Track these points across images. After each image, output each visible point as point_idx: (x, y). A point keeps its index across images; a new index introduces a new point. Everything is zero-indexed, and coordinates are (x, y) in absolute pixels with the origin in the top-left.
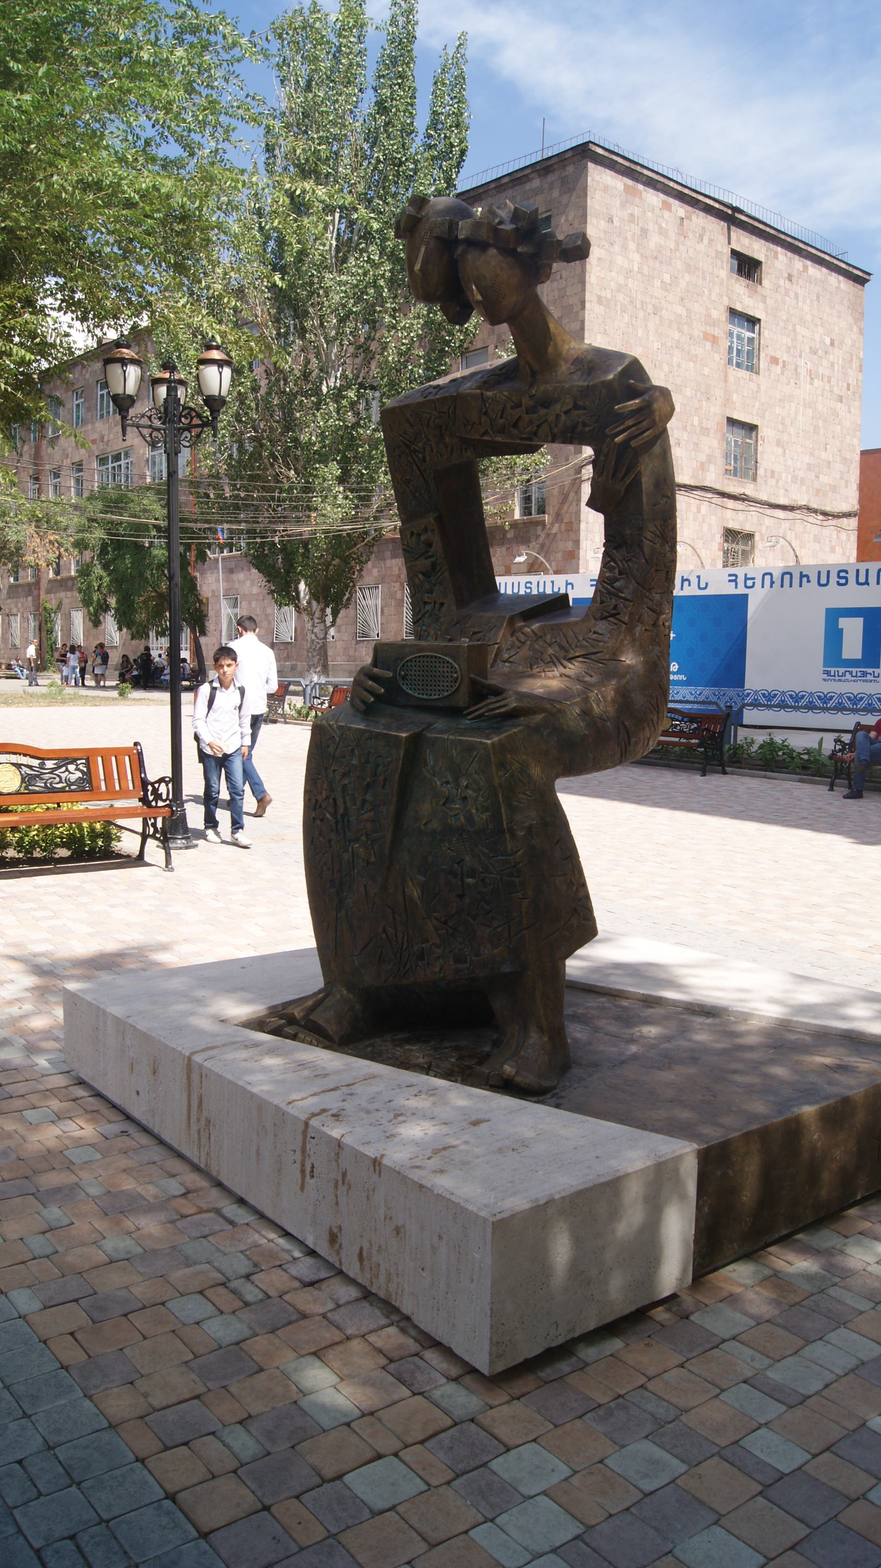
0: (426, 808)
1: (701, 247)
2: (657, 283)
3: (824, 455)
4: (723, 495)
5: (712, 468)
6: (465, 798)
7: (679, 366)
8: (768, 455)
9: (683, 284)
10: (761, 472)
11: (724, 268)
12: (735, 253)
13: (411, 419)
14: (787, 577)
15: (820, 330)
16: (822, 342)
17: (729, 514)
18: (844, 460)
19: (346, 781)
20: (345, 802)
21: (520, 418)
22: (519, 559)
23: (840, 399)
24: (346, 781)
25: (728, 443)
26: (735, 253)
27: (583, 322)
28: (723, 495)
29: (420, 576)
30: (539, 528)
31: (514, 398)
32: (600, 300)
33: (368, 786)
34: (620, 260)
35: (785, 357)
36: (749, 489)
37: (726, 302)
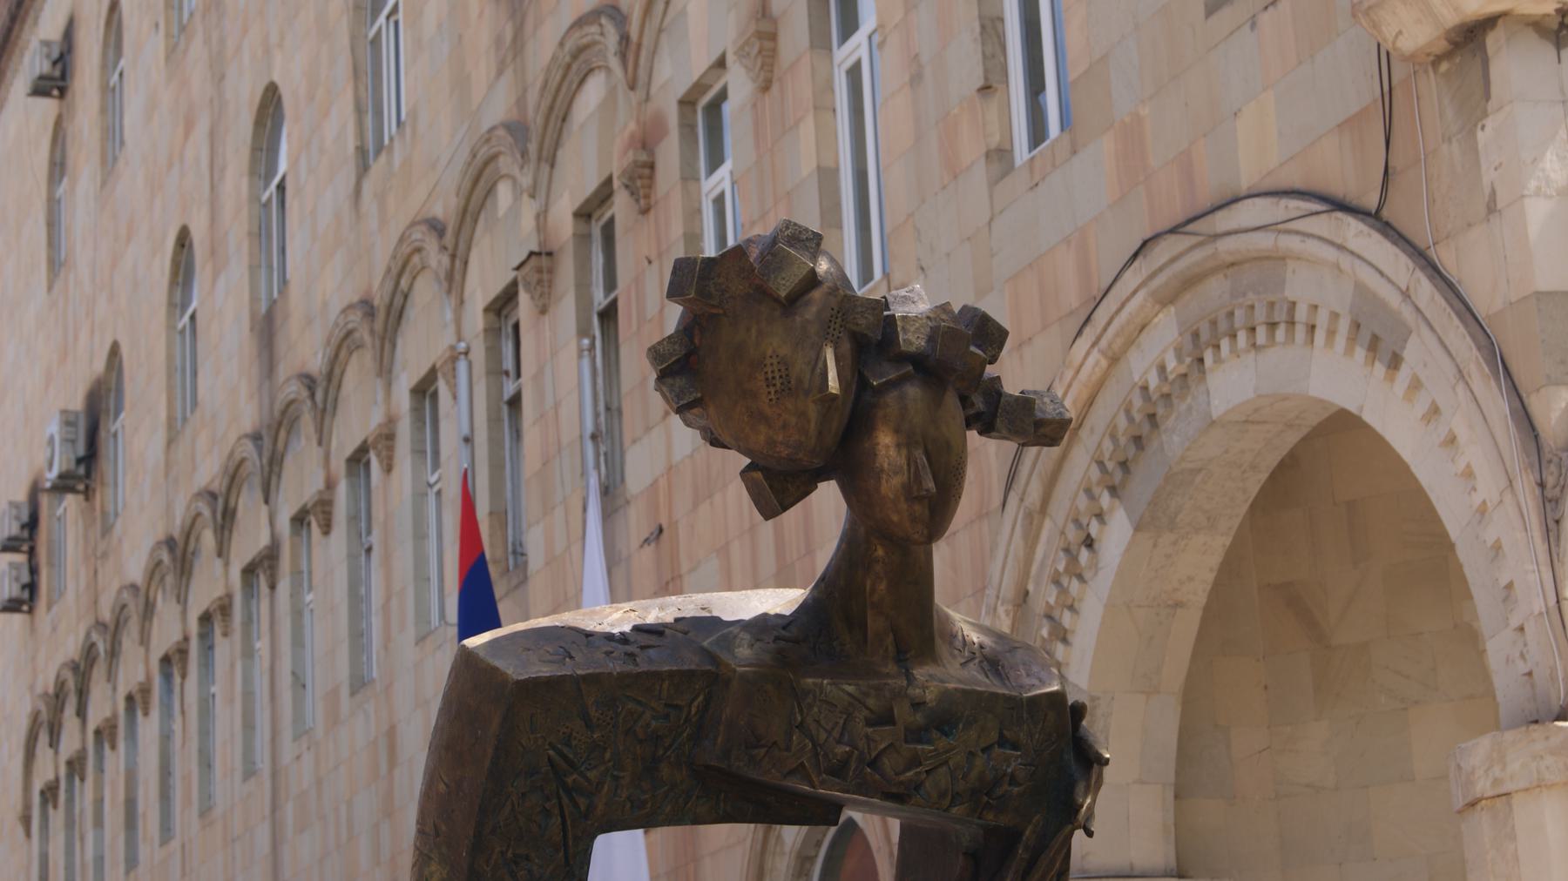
13: (593, 713)
21: (891, 745)
31: (871, 702)
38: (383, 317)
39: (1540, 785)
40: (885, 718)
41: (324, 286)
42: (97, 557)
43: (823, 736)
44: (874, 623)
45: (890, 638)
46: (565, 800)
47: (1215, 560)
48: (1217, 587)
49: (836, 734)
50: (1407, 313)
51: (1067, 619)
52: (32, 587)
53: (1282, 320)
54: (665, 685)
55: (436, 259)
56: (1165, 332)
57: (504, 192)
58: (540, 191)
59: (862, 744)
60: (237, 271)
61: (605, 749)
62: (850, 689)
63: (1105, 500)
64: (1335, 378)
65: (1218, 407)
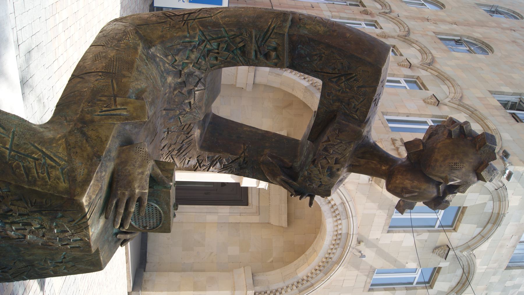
13: (363, 89)
21: (329, 162)
29: (241, 45)
31: (342, 159)
40: (337, 162)
43: (336, 147)
45: (357, 164)
46: (336, 75)
49: (336, 150)
54: (364, 110)
59: (332, 156)
61: (350, 90)
62: (347, 155)
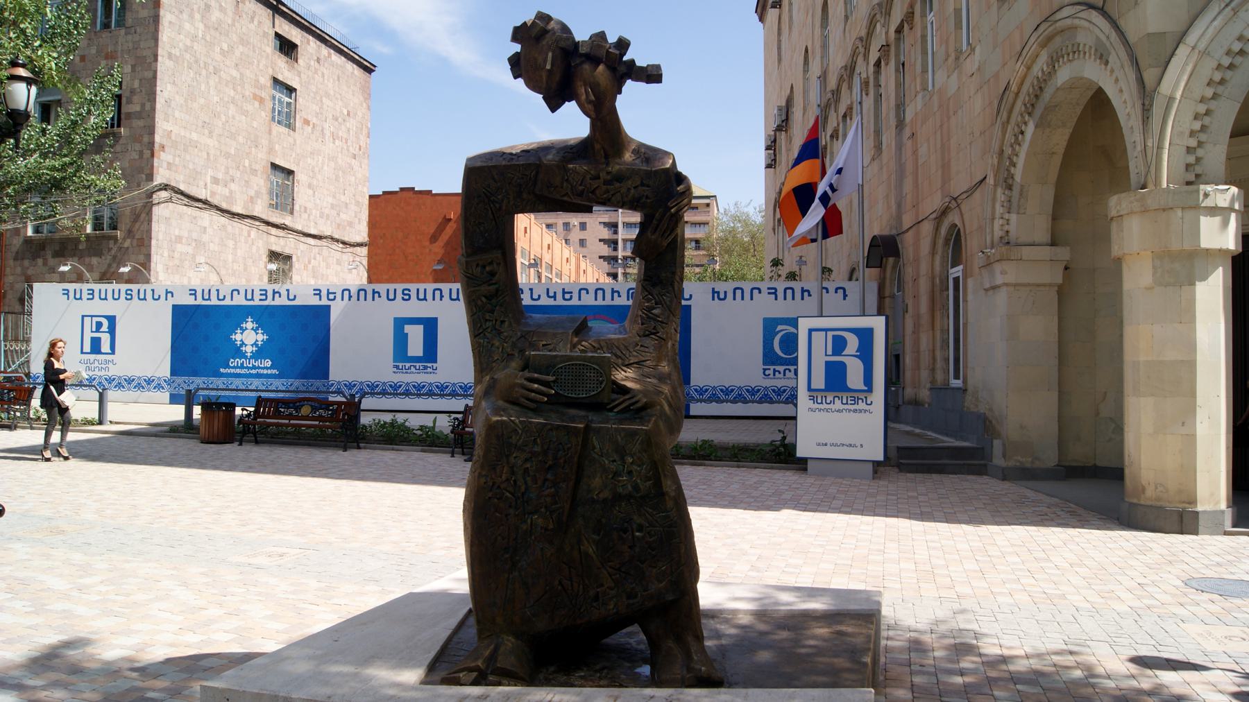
0: (597, 482)
1: (252, 26)
2: (217, 49)
3: (343, 198)
4: (268, 223)
5: (259, 201)
6: (630, 473)
7: (234, 117)
8: (302, 195)
9: (237, 53)
10: (297, 207)
11: (270, 46)
12: (277, 35)
14: (362, 293)
15: (340, 103)
16: (341, 112)
17: (273, 239)
18: (358, 204)
19: (528, 465)
20: (526, 483)
22: (123, 270)
23: (354, 157)
24: (528, 465)
25: (272, 183)
26: (277, 35)
27: (155, 72)
28: (268, 223)
30: (112, 242)
32: (170, 56)
33: (550, 468)
34: (187, 26)
35: (314, 120)
36: (288, 221)
37: (270, 72)
38: (850, 69)
39: (1131, 213)
41: (838, 61)
42: (788, 150)
44: (597, 146)
47: (1067, 137)
48: (1068, 146)
50: (1108, 44)
51: (1015, 159)
52: (775, 160)
53: (1076, 51)
55: (861, 50)
56: (1044, 57)
57: (878, 25)
58: (886, 25)
60: (818, 59)
63: (1027, 118)
64: (1092, 71)
65: (1059, 83)
